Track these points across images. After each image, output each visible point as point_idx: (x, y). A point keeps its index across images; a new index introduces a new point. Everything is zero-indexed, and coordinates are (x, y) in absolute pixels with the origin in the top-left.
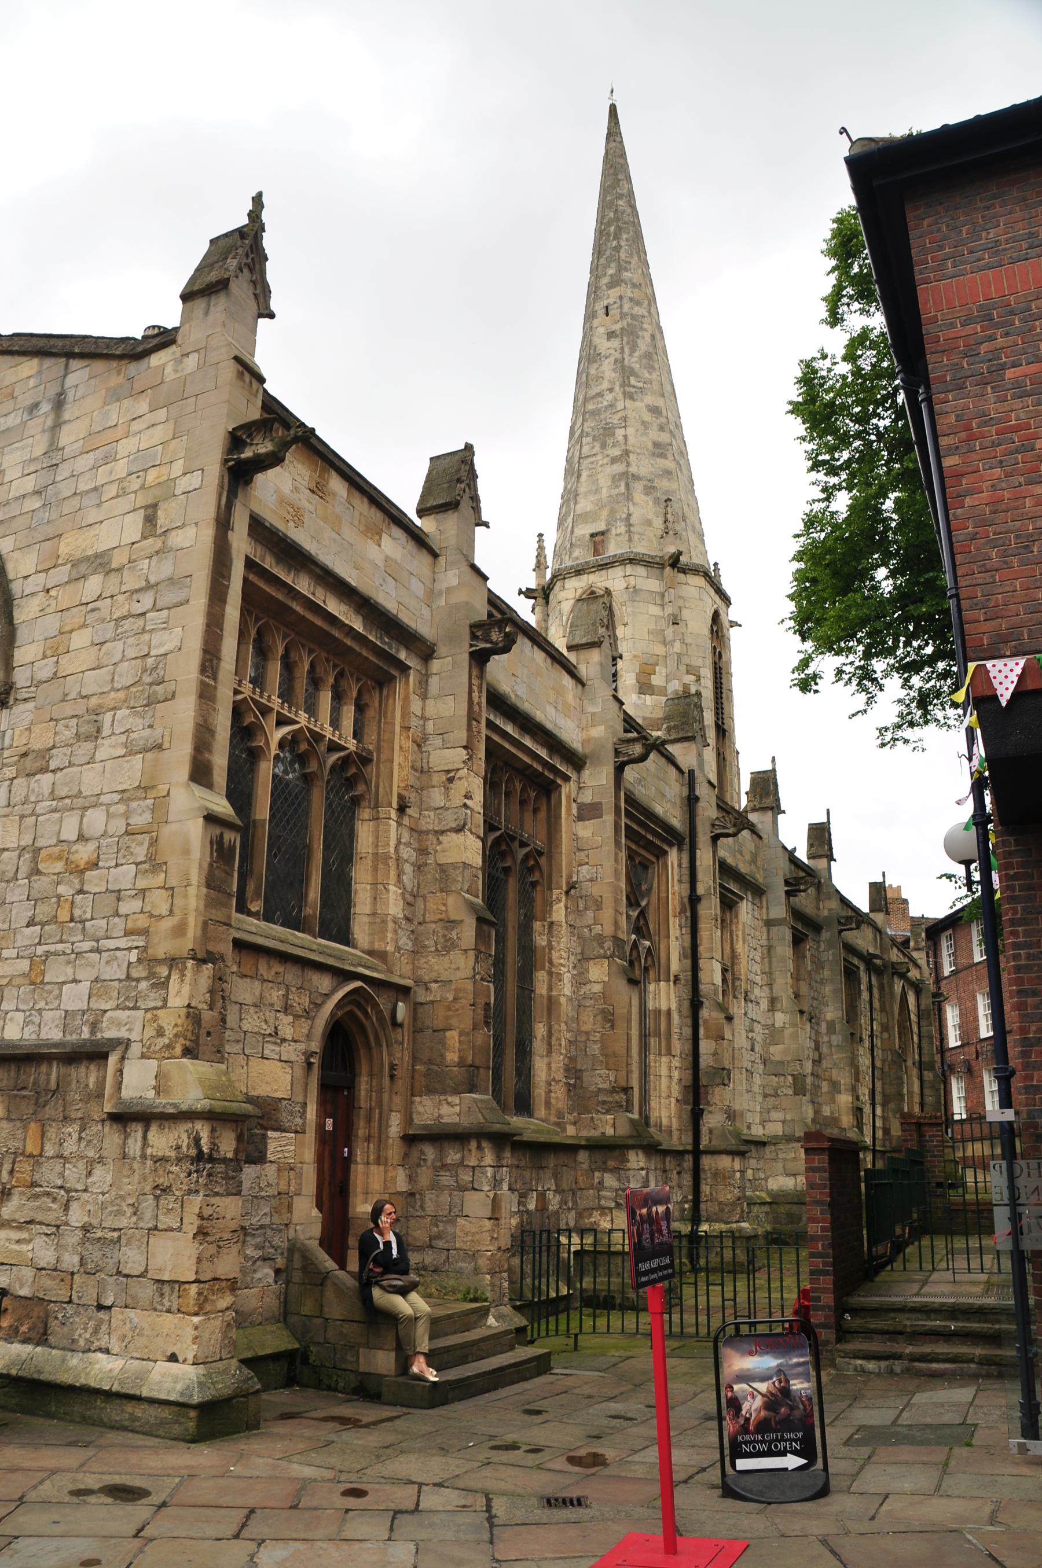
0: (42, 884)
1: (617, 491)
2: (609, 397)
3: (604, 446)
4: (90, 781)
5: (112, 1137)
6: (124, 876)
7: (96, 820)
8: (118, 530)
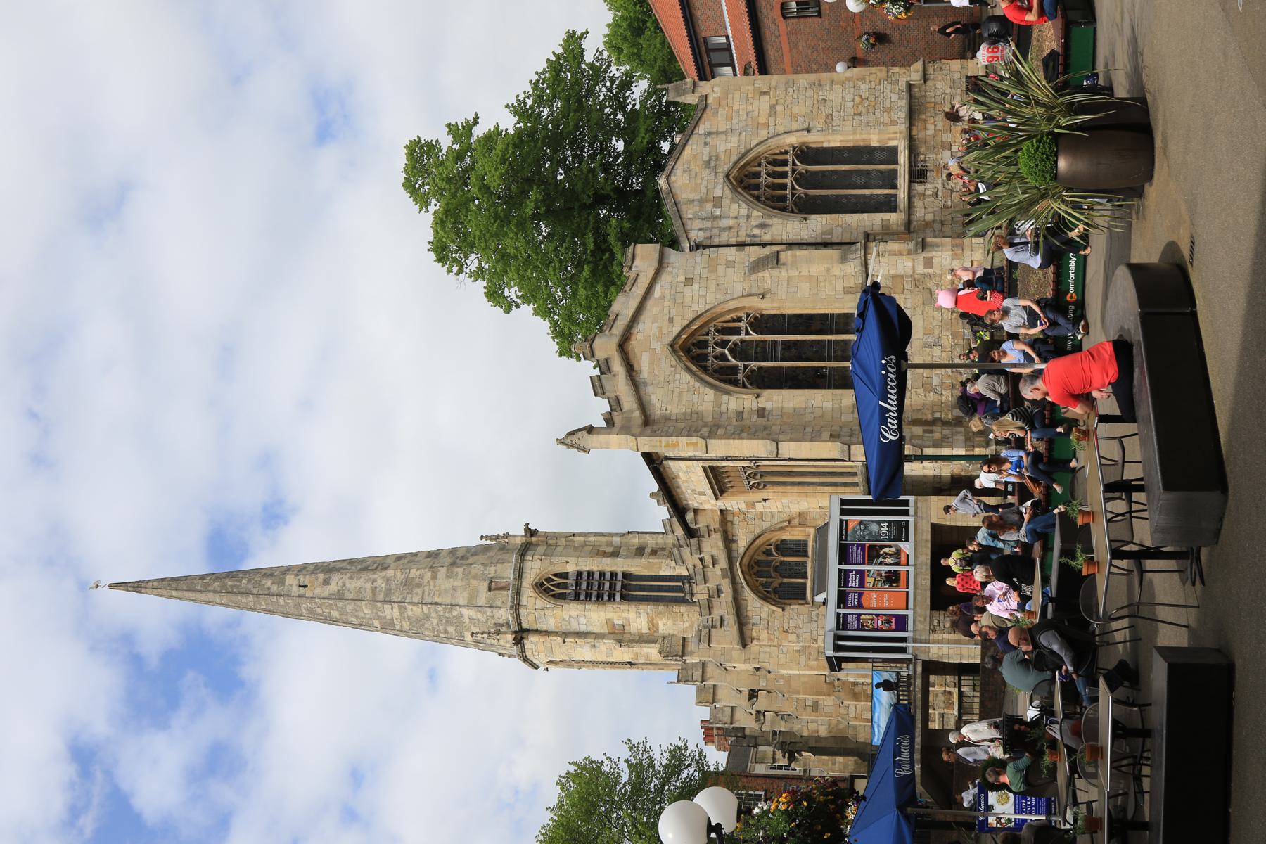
0: (864, 111)
1: (460, 576)
2: (379, 582)
3: (419, 585)
4: (838, 100)
5: (930, 83)
6: (865, 87)
7: (849, 98)
8: (765, 102)
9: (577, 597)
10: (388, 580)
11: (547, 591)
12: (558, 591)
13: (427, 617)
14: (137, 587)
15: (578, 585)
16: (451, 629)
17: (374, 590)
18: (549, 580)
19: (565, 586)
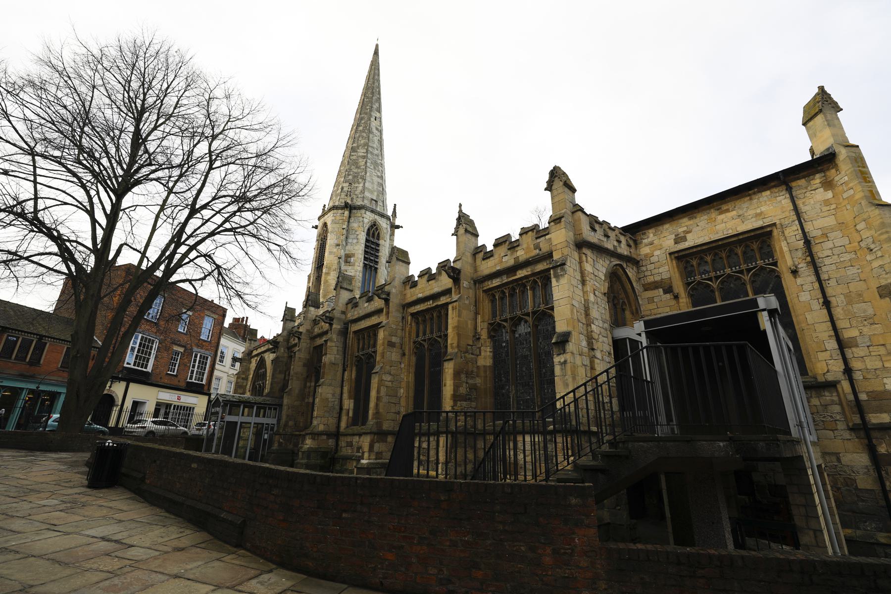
9: (367, 241)
10: (377, 155)
11: (372, 227)
12: (371, 232)
13: (358, 167)
14: (376, 53)
15: (373, 243)
16: (350, 177)
17: (373, 147)
18: (377, 229)
19: (373, 237)
